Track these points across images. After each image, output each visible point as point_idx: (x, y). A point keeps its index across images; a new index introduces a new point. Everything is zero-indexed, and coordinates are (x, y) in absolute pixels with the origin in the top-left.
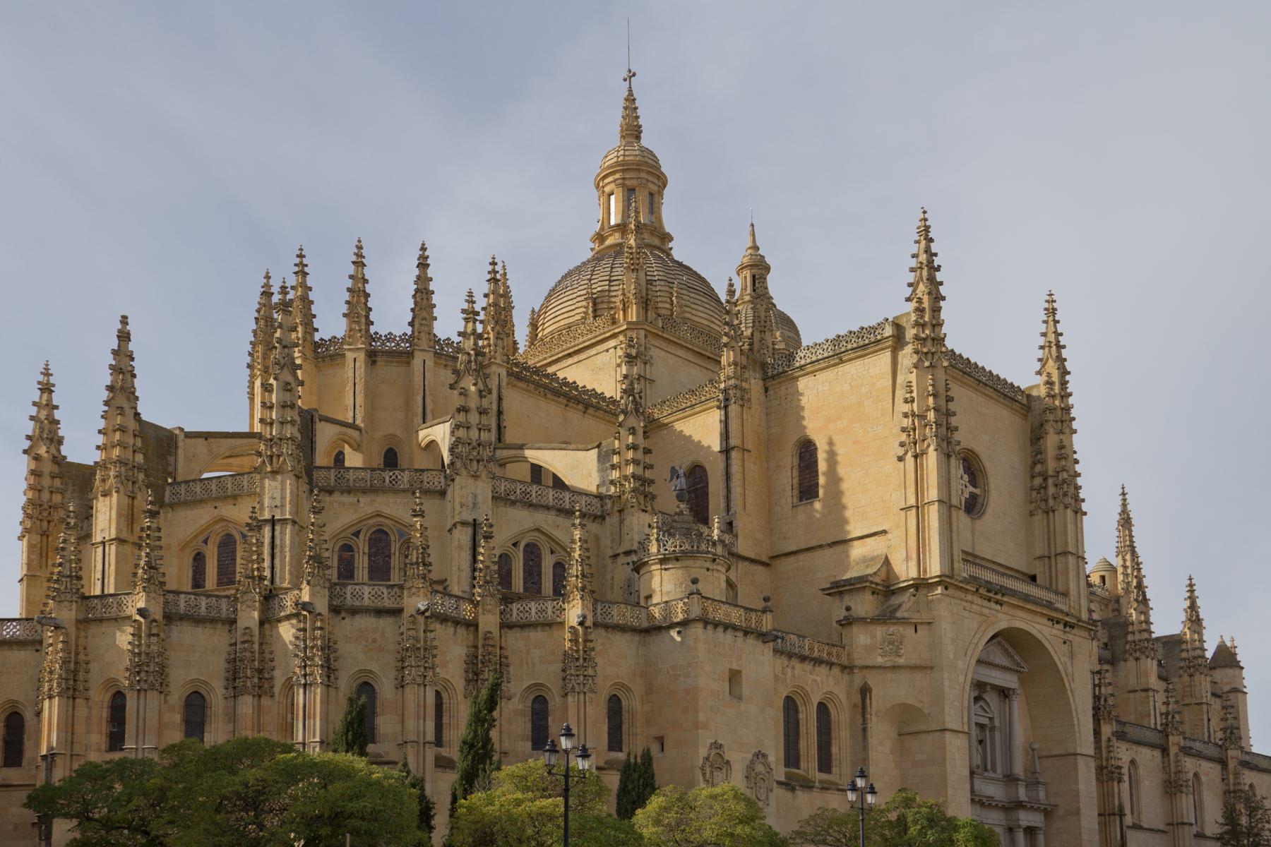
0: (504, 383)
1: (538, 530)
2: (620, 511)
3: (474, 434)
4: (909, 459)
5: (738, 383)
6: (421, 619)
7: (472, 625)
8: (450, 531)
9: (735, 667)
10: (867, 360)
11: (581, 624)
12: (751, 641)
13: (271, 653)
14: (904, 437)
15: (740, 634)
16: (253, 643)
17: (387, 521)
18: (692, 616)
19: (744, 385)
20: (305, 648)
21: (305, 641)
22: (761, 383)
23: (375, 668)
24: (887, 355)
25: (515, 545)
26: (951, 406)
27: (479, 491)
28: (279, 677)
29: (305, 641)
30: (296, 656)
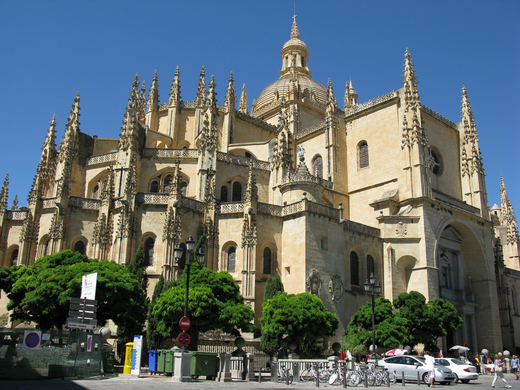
1: (240, 176)
2: (277, 168)
3: (209, 134)
6: (174, 209)
7: (201, 214)
8: (198, 174)
9: (324, 234)
11: (250, 213)
12: (332, 223)
13: (113, 225)
14: (404, 139)
15: (327, 219)
16: (105, 221)
18: (303, 209)
20: (123, 221)
21: (123, 218)
23: (155, 232)
24: (395, 106)
25: (229, 182)
28: (114, 235)
29: (123, 218)
30: (118, 224)
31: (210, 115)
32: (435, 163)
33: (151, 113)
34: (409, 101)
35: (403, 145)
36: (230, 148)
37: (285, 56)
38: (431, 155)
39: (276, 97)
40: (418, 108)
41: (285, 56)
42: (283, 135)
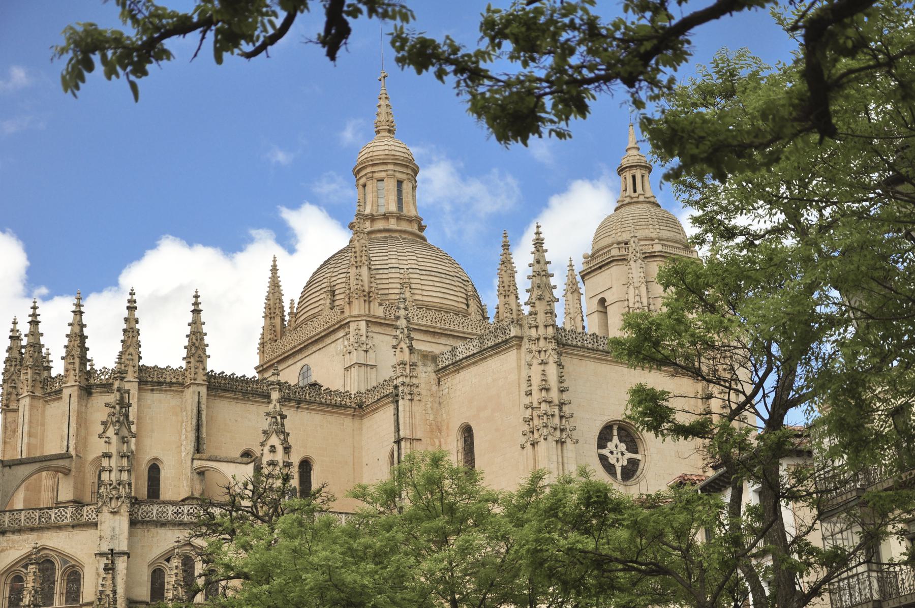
0: (204, 400)
4: (528, 445)
5: (407, 380)
10: (503, 357)
14: (526, 428)
17: (52, 553)
19: (414, 381)
22: (433, 376)
26: (565, 396)
27: (117, 524)
31: (114, 439)
32: (629, 455)
33: (28, 400)
34: (534, 348)
35: (523, 440)
36: (197, 463)
37: (362, 181)
38: (616, 439)
39: (329, 301)
40: (551, 361)
41: (362, 181)
42: (273, 449)
